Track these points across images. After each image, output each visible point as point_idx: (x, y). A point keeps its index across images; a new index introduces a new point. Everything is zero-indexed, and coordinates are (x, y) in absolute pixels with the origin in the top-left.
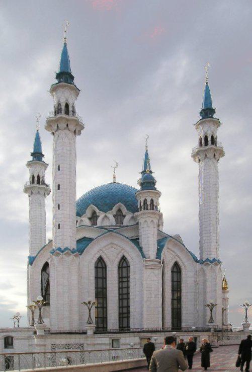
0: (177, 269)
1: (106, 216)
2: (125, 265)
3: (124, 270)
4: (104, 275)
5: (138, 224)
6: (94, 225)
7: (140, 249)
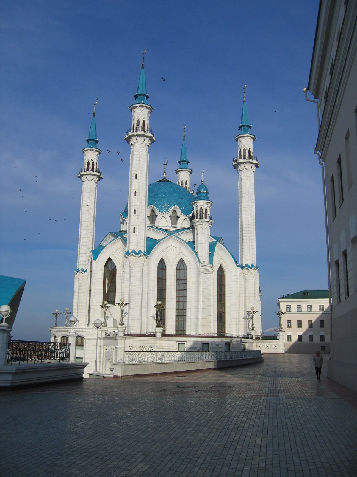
2: (182, 268)
7: (196, 253)
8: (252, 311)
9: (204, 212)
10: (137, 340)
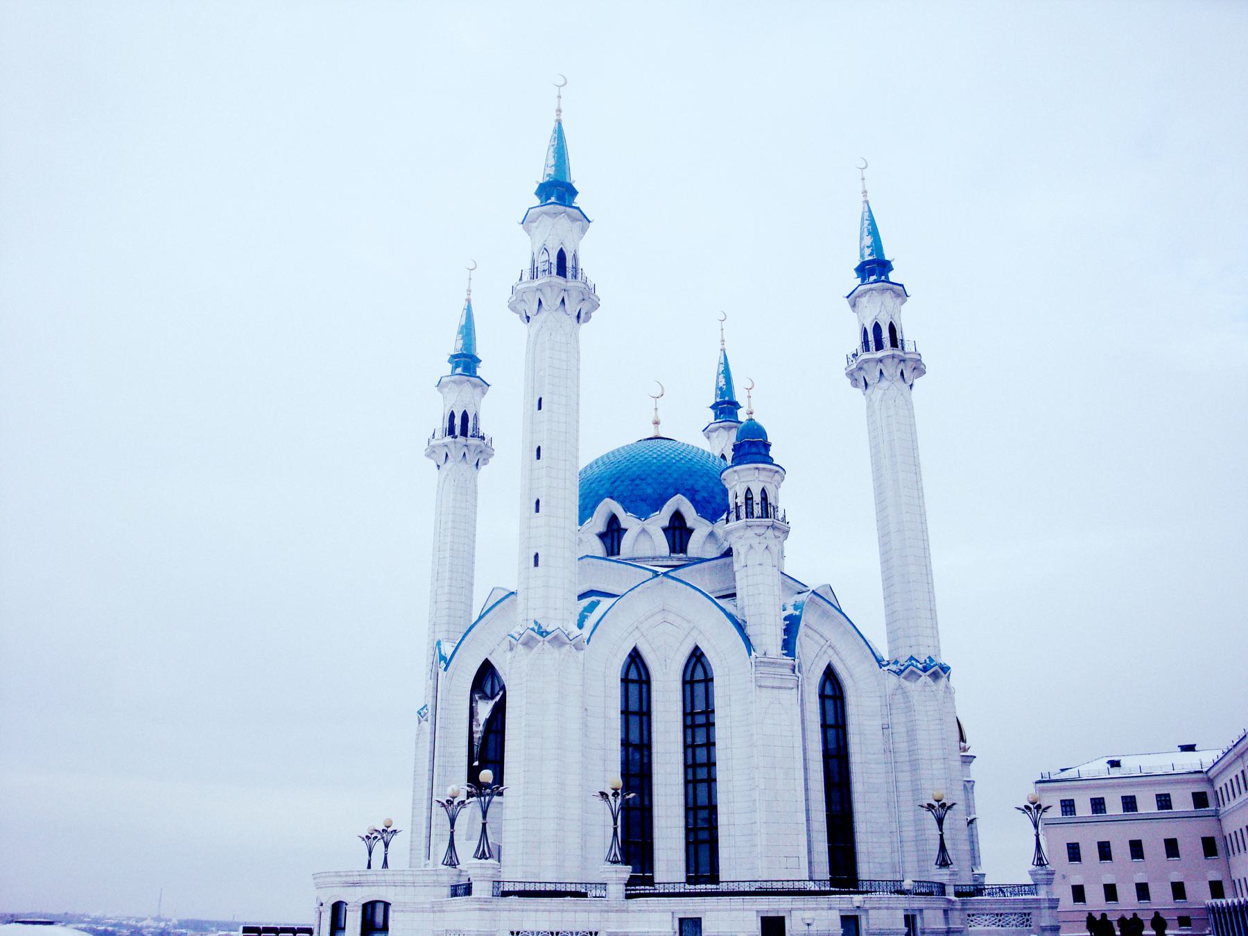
0: (834, 689)
1: (644, 531)
2: (699, 675)
3: (700, 689)
4: (644, 704)
5: (728, 553)
6: (612, 554)
8: (936, 804)
9: (757, 498)
10: (537, 911)
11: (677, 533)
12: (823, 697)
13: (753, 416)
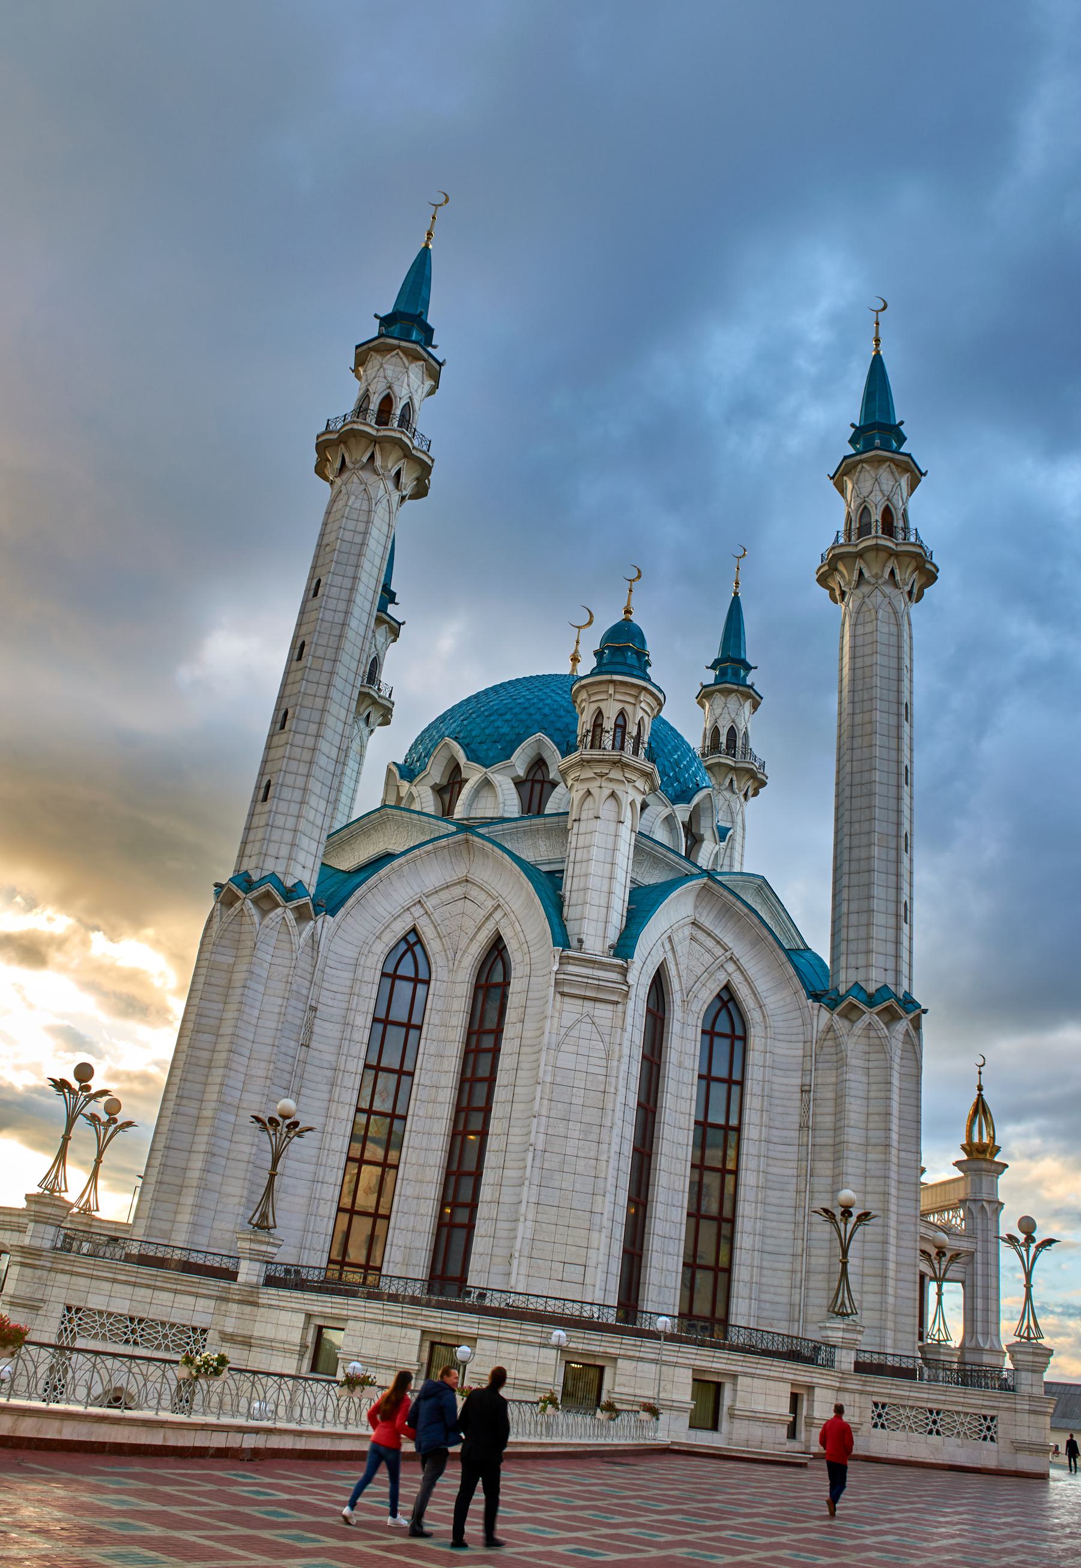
1: (486, 783)
9: (609, 724)
10: (114, 1281)
11: (537, 787)
12: (709, 1033)
13: (632, 617)
